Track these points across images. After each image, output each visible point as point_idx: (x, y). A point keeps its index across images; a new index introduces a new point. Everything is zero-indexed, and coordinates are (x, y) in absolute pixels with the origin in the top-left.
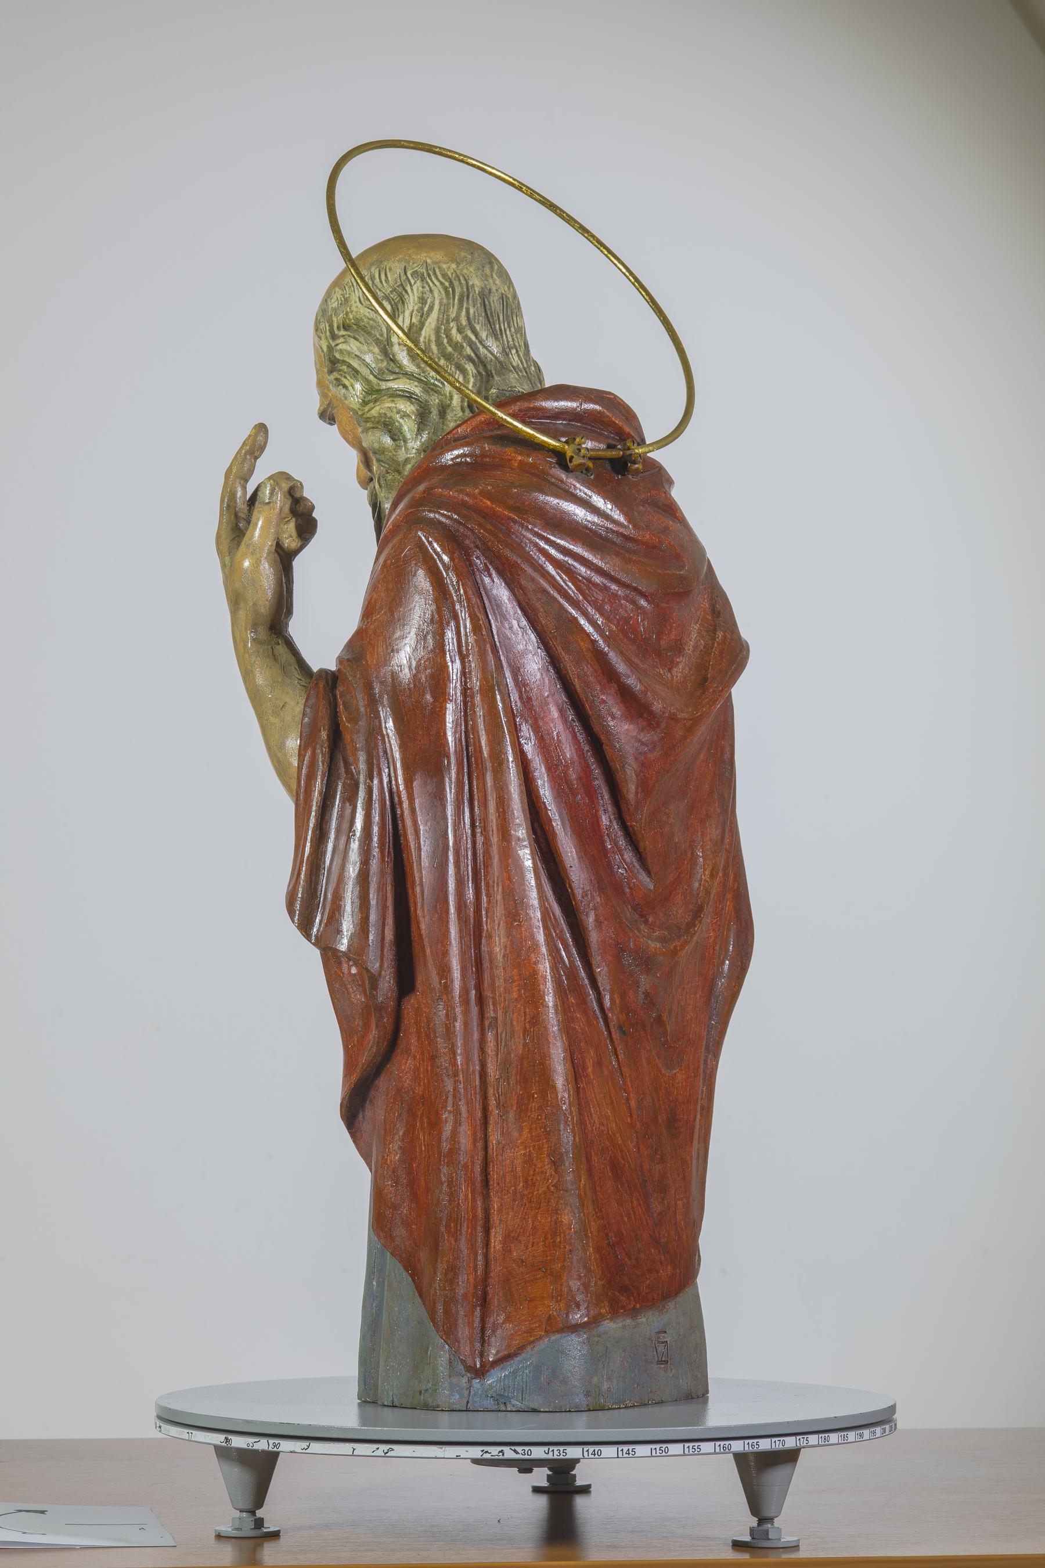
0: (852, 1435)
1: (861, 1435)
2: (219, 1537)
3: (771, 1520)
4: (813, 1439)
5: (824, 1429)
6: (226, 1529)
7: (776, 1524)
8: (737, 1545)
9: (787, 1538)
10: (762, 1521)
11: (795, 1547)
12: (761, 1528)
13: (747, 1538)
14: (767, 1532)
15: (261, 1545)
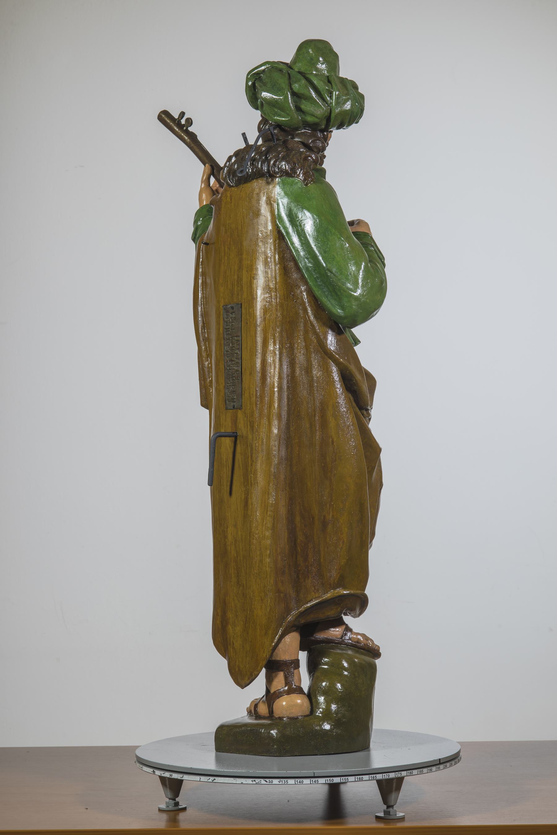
0: (425, 770)
1: (431, 770)
2: (160, 810)
3: (392, 806)
4: (404, 773)
5: (410, 768)
6: (163, 806)
7: (395, 809)
8: (377, 817)
9: (400, 814)
10: (388, 807)
11: (402, 819)
12: (388, 810)
13: (382, 814)
14: (389, 812)
15: (178, 814)
